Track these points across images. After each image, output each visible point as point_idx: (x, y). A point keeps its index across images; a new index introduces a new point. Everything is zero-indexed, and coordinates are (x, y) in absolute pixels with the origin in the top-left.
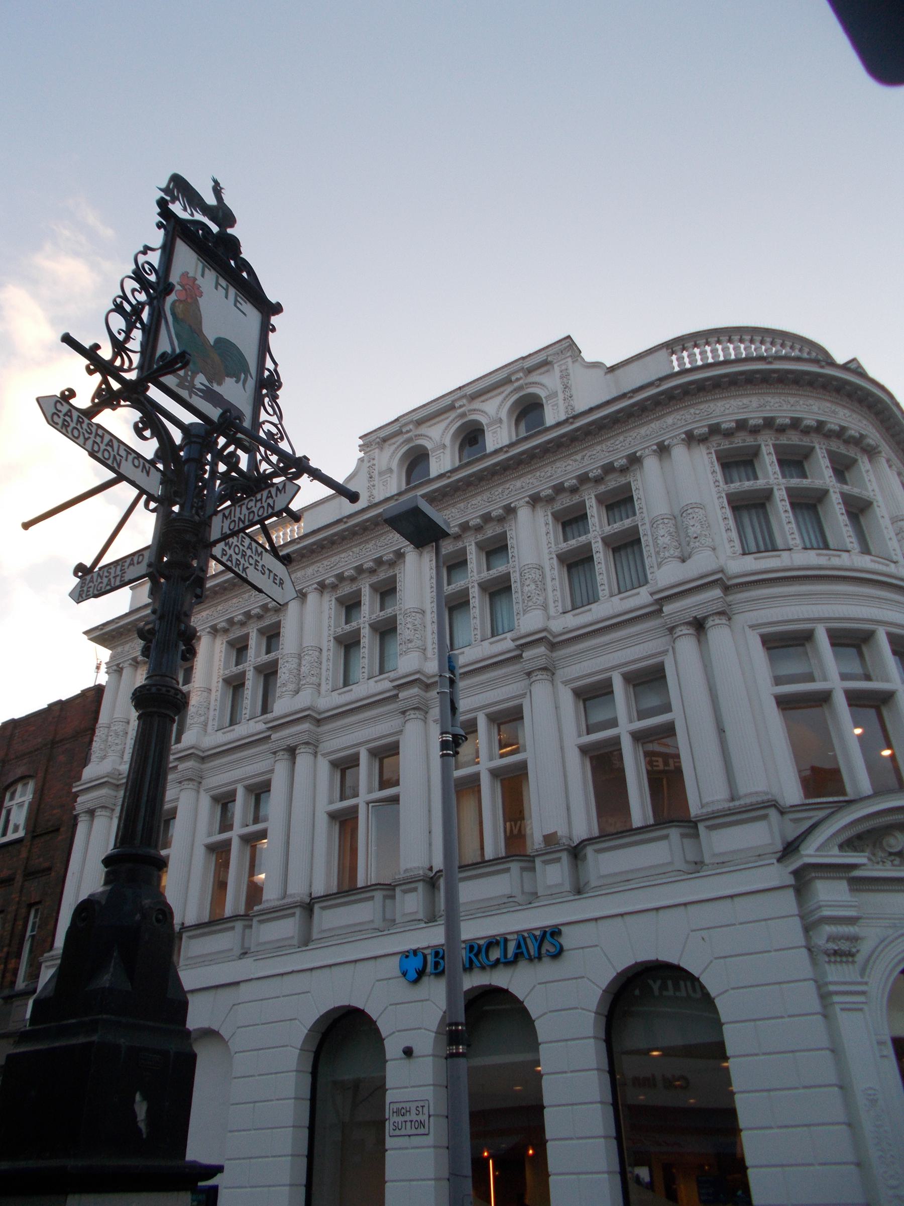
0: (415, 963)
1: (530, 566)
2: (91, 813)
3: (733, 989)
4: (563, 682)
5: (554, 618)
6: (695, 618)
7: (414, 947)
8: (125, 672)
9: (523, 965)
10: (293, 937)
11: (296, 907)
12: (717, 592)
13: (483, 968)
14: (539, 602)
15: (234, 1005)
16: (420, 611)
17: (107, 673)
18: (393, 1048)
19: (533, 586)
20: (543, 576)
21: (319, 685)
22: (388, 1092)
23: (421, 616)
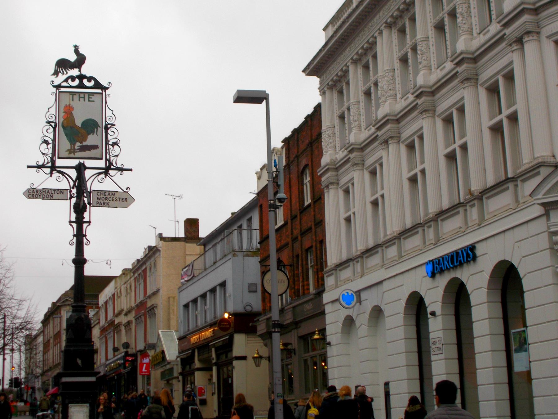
0: (430, 266)
1: (459, 3)
2: (327, 187)
3: (528, 273)
4: (481, 85)
5: (475, 38)
6: (516, 37)
7: (431, 259)
8: (327, 92)
9: (465, 265)
10: (396, 256)
11: (395, 239)
12: (526, 17)
13: (453, 268)
14: (464, 29)
15: (383, 293)
16: (425, 39)
17: (320, 95)
18: (429, 310)
19: (461, 18)
20: (469, 7)
21: (396, 95)
22: (431, 334)
23: (426, 42)
